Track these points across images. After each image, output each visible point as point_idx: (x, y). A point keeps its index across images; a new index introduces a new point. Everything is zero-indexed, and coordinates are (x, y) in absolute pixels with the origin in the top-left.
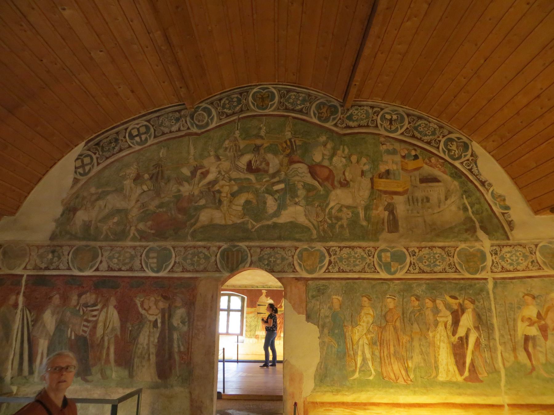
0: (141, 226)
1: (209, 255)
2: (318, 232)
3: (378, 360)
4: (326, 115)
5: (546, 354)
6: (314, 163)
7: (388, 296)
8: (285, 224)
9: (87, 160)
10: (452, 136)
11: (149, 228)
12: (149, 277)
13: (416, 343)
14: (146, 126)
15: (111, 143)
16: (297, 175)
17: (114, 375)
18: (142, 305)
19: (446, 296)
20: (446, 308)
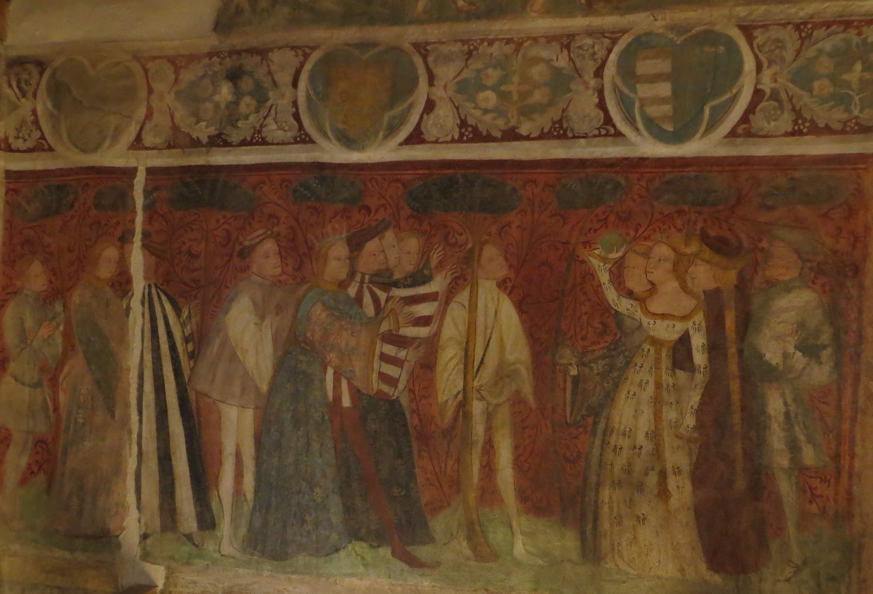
12: (642, 161)
17: (520, 549)
18: (618, 279)
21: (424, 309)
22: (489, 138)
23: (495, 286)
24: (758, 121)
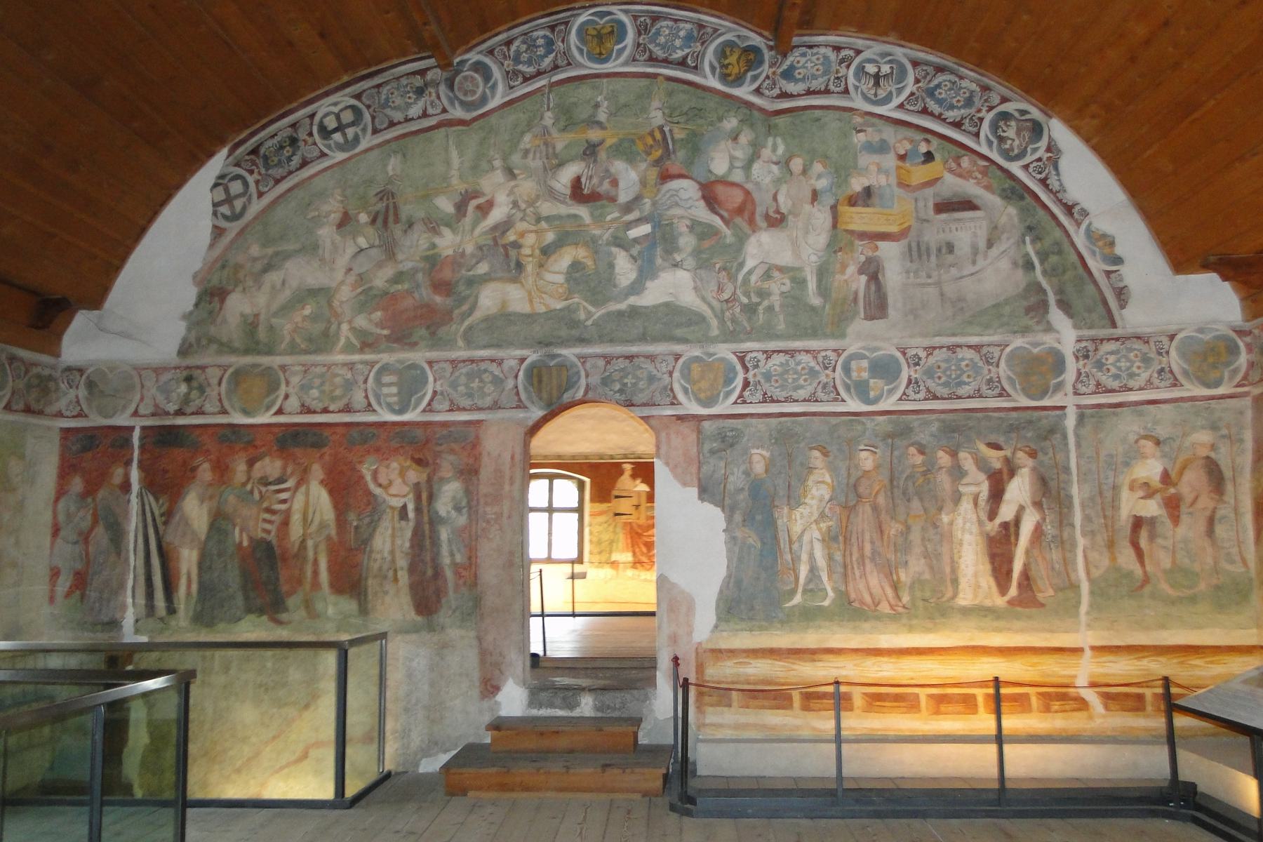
0: (361, 322)
1: (501, 375)
2: (722, 321)
3: (840, 569)
4: (736, 70)
5: (1174, 552)
6: (713, 178)
7: (862, 447)
8: (656, 307)
9: (236, 187)
10: (1009, 107)
11: (377, 325)
12: (385, 424)
13: (915, 536)
14: (352, 107)
15: (282, 148)
16: (677, 204)
19: (978, 442)
20: (980, 468)
21: (284, 496)
22: (315, 412)
24: (435, 405)
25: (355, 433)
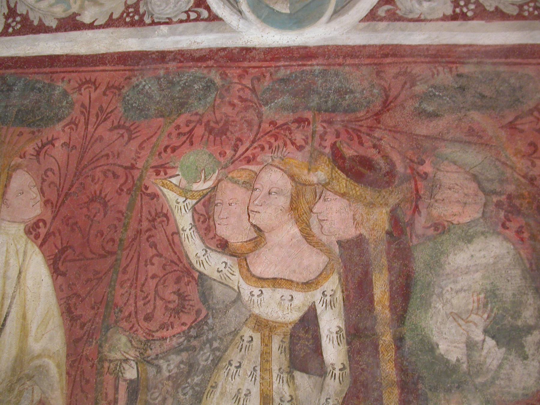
18: (205, 221)
22: (42, 29)
23: (22, 233)
25: (147, 82)
